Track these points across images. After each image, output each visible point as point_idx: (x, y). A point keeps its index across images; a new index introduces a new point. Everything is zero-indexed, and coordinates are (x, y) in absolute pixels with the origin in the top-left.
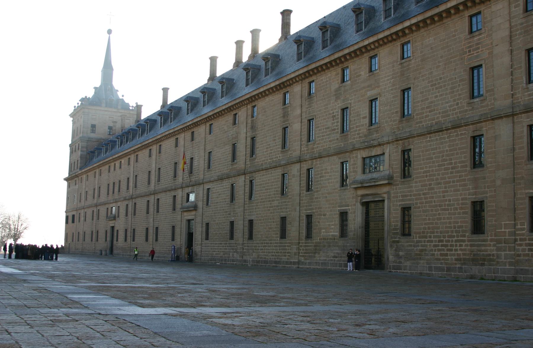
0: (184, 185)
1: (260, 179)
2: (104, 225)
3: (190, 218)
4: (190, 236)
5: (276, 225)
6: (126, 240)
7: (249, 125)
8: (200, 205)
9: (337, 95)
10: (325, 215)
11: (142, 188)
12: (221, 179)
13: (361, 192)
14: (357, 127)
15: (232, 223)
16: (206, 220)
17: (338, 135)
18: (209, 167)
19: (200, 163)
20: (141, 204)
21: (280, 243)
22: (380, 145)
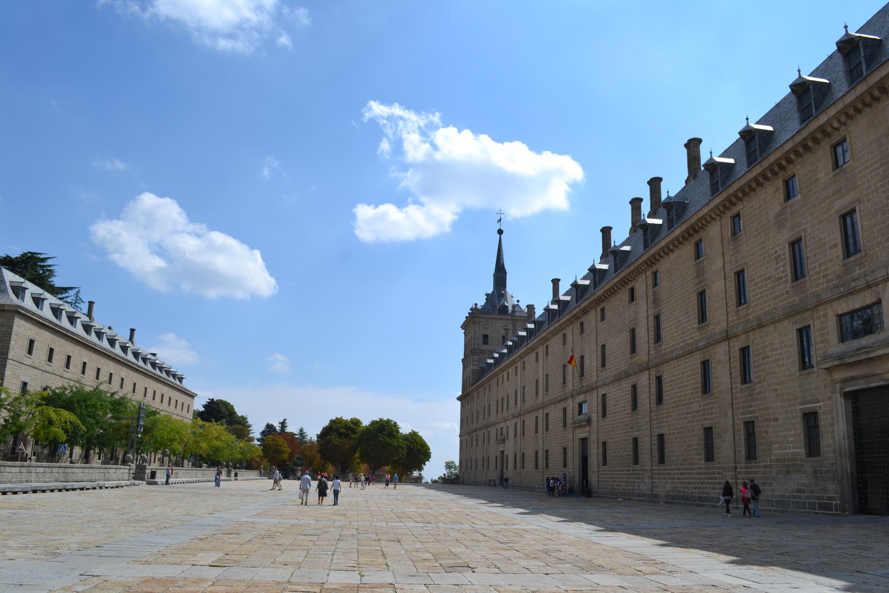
0: (575, 393)
1: (669, 373)
2: (494, 450)
3: (583, 435)
4: (585, 460)
5: (697, 441)
6: (515, 468)
7: (651, 298)
8: (594, 417)
9: (780, 221)
10: (776, 420)
11: (530, 402)
12: (618, 379)
13: (839, 375)
14: (820, 265)
15: (635, 440)
16: (602, 438)
17: (788, 286)
18: (604, 365)
19: (592, 362)
20: (530, 420)
21: (706, 468)
22: (869, 286)
